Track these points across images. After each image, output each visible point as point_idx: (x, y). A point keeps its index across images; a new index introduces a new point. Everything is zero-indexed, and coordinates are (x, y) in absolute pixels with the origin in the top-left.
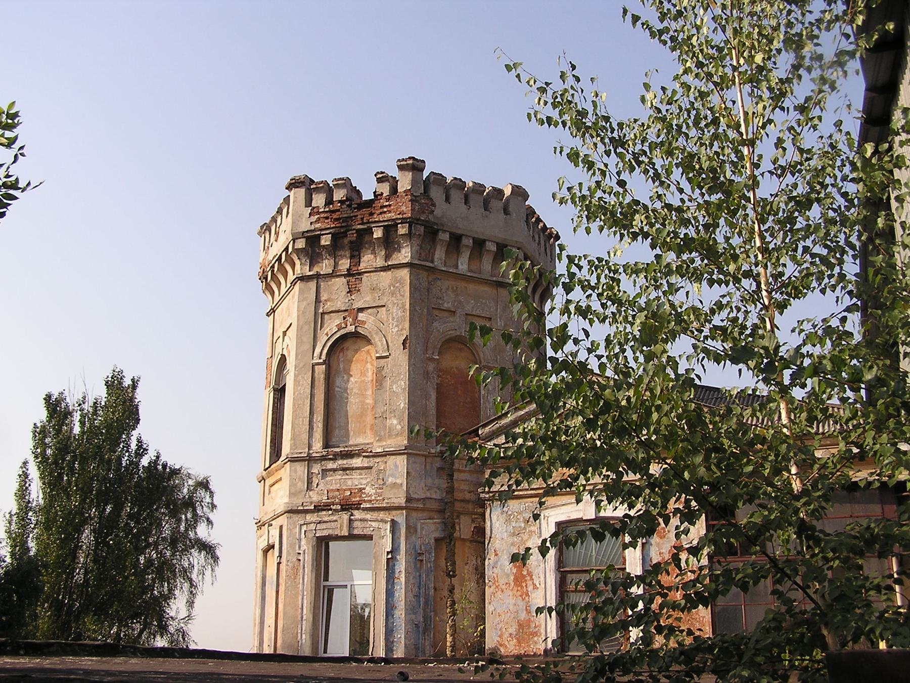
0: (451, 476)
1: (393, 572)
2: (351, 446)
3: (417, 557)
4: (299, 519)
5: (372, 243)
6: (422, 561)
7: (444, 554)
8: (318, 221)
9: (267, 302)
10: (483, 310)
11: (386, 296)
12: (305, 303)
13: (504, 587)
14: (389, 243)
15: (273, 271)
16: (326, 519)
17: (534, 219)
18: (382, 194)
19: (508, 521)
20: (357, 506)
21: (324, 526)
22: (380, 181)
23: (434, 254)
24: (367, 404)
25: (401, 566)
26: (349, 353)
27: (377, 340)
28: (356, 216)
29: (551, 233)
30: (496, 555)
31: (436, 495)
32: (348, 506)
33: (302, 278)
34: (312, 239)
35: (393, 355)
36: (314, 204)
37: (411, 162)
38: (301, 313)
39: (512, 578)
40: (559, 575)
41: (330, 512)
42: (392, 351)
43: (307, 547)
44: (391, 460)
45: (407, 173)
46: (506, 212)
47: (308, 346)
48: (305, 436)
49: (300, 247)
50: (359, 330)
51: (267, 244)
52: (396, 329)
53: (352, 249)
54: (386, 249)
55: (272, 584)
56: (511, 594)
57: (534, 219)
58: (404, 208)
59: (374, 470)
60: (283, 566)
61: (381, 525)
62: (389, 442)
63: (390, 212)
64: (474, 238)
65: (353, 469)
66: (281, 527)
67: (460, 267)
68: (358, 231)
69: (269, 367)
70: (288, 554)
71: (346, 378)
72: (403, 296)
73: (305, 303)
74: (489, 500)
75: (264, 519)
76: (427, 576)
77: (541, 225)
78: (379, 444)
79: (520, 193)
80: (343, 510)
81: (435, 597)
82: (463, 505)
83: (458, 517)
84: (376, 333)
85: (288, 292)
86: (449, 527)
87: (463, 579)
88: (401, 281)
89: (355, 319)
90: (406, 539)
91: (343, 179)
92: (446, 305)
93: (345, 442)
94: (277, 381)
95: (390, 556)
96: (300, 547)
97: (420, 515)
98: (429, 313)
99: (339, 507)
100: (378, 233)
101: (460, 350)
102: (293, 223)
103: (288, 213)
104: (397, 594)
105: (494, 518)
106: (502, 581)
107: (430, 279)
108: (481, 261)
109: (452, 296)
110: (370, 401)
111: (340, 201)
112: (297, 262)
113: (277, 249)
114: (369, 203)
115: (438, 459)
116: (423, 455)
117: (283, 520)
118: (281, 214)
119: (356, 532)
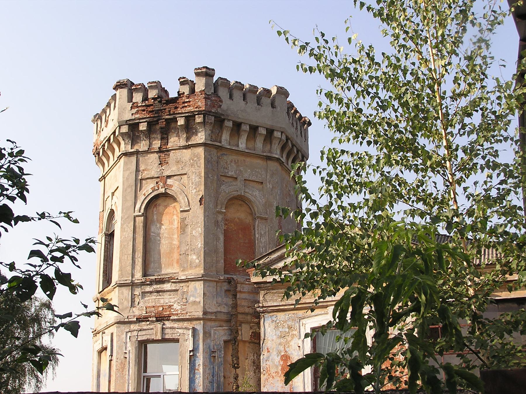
0: (235, 296)
1: (194, 365)
2: (163, 275)
3: (211, 354)
4: (125, 328)
5: (176, 129)
6: (215, 357)
7: (230, 352)
8: (137, 112)
9: (99, 171)
10: (257, 176)
11: (187, 167)
12: (128, 172)
13: (274, 375)
14: (189, 128)
15: (104, 149)
16: (145, 328)
17: (293, 111)
18: (184, 93)
19: (277, 327)
20: (168, 318)
21: (144, 333)
22: (182, 83)
23: (221, 137)
24: (174, 244)
25: (200, 361)
26: (161, 208)
27: (181, 198)
28: (165, 109)
29: (305, 121)
30: (268, 352)
31: (225, 310)
32: (160, 318)
33: (126, 154)
34: (133, 126)
35: (192, 209)
36: (134, 100)
37: (204, 70)
38: (126, 180)
39: (280, 368)
41: (148, 323)
42: (192, 207)
43: (131, 348)
44: (192, 284)
45: (201, 78)
46: (273, 106)
47: (131, 203)
48: (129, 268)
49: (124, 131)
50: (168, 191)
51: (99, 129)
52: (195, 191)
53: (162, 133)
54: (187, 133)
55: (105, 376)
56: (279, 379)
57: (293, 111)
58: (199, 104)
59: (179, 292)
60: (113, 363)
61: (185, 331)
62: (190, 272)
63: (190, 106)
64: (250, 125)
65: (164, 291)
66: (112, 334)
67: (240, 146)
68: (166, 120)
69: (101, 218)
70: (118, 353)
71: (158, 226)
72: (200, 167)
73: (128, 172)
74: (263, 313)
75: (99, 329)
76: (219, 368)
77: (298, 115)
78: (182, 273)
79: (283, 92)
80: (157, 321)
81: (224, 383)
82: (244, 316)
83: (240, 325)
84: (181, 194)
85: (115, 164)
86: (234, 332)
87: (244, 370)
88: (198, 156)
89: (165, 183)
90: (204, 341)
91: (155, 82)
92: (230, 174)
93: (158, 272)
94: (108, 228)
95: (192, 354)
96: (126, 348)
97: (213, 324)
98: (218, 180)
99: (154, 319)
100: (181, 122)
101: (241, 205)
102: (119, 114)
103: (115, 107)
104: (197, 381)
105: (267, 325)
106: (273, 370)
107: (219, 154)
108: (255, 141)
109: (235, 167)
110: (176, 242)
111: (153, 99)
112: (122, 143)
113: (107, 132)
114: (174, 100)
115: (226, 284)
116: (215, 281)
117: (114, 329)
118: (110, 107)
119: (167, 337)
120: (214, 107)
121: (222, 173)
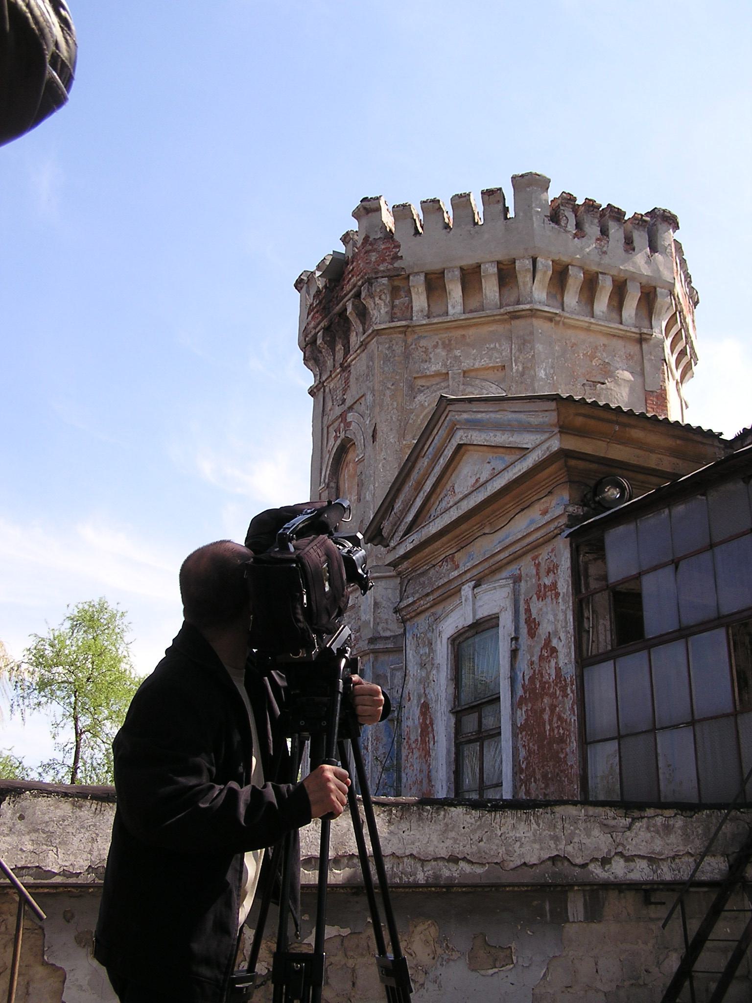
40: (453, 720)
67: (451, 311)
120: (384, 260)
121: (418, 372)
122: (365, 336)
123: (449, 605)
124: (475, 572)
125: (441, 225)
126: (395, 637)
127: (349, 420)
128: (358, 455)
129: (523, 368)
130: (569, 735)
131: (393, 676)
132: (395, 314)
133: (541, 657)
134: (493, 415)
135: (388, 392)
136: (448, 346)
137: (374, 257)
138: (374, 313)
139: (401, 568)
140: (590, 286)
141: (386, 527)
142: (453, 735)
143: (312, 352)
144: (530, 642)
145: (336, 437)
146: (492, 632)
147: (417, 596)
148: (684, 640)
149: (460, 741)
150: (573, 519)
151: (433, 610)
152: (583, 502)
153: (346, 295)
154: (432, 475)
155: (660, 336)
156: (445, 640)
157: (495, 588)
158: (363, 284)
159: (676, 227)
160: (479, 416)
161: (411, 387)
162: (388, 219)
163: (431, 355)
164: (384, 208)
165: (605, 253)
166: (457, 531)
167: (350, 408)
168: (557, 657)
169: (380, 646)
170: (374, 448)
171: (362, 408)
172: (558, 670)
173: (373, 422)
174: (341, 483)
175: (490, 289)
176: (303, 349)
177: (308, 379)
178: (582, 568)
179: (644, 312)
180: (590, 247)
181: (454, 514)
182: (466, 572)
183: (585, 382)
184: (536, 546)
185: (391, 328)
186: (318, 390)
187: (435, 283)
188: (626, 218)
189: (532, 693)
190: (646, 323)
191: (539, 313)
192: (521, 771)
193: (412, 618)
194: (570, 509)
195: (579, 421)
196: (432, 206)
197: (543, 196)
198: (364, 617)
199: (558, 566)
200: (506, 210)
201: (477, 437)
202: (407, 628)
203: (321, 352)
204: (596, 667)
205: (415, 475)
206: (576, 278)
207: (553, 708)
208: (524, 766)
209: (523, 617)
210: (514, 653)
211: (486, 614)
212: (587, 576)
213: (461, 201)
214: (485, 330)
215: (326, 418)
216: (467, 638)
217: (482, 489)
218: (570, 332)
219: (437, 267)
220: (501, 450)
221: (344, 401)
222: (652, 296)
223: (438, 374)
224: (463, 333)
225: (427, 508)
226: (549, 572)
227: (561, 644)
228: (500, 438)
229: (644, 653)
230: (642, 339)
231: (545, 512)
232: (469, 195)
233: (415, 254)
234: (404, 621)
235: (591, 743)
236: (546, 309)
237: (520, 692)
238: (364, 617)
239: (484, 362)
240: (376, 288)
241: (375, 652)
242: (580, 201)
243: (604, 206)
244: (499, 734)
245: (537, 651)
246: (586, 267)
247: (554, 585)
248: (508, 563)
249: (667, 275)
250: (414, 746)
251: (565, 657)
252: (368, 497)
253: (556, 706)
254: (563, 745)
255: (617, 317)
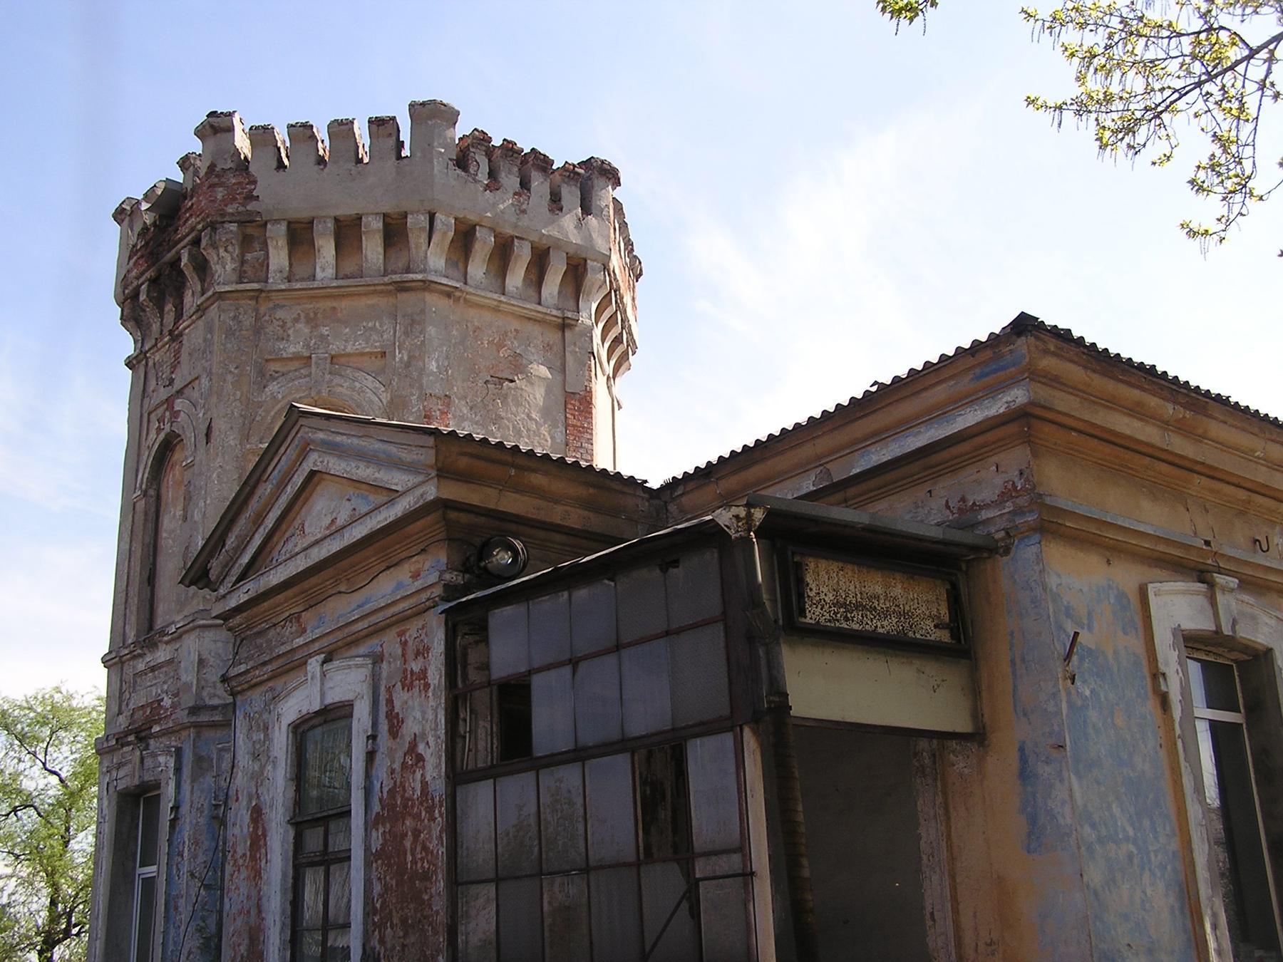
40: (292, 834)
67: (319, 274)
90: (193, 781)
120: (234, 199)
121: (270, 353)
122: (203, 298)
123: (292, 680)
124: (325, 642)
125: (313, 159)
126: (225, 706)
127: (177, 408)
128: (186, 458)
129: (410, 357)
130: (435, 872)
131: (220, 759)
132: (245, 272)
133: (404, 764)
134: (355, 441)
135: (229, 378)
136: (312, 321)
137: (220, 193)
138: (217, 268)
139: (232, 623)
140: (503, 253)
141: (215, 567)
142: (291, 854)
143: (133, 309)
144: (390, 743)
145: (159, 430)
146: (343, 723)
147: (251, 664)
148: (580, 764)
149: (300, 863)
150: (451, 591)
151: (270, 684)
152: (465, 568)
153: (181, 240)
154: (277, 506)
155: (588, 322)
156: (284, 728)
157: (349, 667)
158: (204, 229)
159: (617, 183)
160: (339, 439)
161: (261, 373)
162: (242, 143)
163: (290, 332)
164: (238, 127)
165: (524, 212)
166: (306, 584)
167: (180, 392)
168: (423, 767)
169: (204, 718)
170: (207, 450)
171: (195, 395)
172: (424, 784)
173: (208, 415)
174: (163, 491)
175: (373, 249)
176: (121, 304)
177: (126, 344)
178: (459, 655)
179: (570, 290)
180: (505, 202)
181: (301, 564)
182: (313, 641)
183: (489, 378)
184: (403, 619)
185: (237, 291)
186: (139, 362)
187: (300, 236)
188: (554, 167)
189: (392, 811)
190: (572, 304)
191: (433, 285)
192: (375, 912)
193: (244, 690)
194: (447, 576)
195: (463, 462)
196: (302, 132)
197: (449, 133)
198: (184, 678)
199: (428, 649)
200: (401, 145)
201: (336, 465)
202: (238, 703)
203: (144, 311)
204: (472, 786)
205: (254, 505)
206: (484, 243)
207: (416, 833)
208: (378, 906)
209: (383, 709)
210: (370, 756)
211: (337, 699)
212: (465, 667)
213: (341, 129)
214: (363, 303)
215: (146, 401)
216: (313, 727)
217: (337, 535)
218: (472, 312)
219: (304, 214)
220: (364, 486)
221: (172, 381)
222: (581, 269)
223: (297, 357)
224: (335, 304)
225: (268, 549)
226: (418, 654)
227: (429, 751)
228: (364, 472)
229: (532, 774)
230: (565, 325)
231: (416, 576)
232: (352, 122)
233: (277, 195)
234: (233, 694)
235: (462, 884)
236: (444, 281)
237: (377, 808)
238: (184, 678)
239: (360, 345)
240: (222, 236)
241: (197, 726)
242: (497, 142)
243: (527, 150)
244: (349, 858)
245: (399, 755)
246: (498, 230)
247: (424, 672)
248: (367, 636)
249: (600, 245)
250: (241, 862)
251: (434, 769)
252: (197, 516)
253: (420, 832)
254: (428, 884)
255: (535, 295)
